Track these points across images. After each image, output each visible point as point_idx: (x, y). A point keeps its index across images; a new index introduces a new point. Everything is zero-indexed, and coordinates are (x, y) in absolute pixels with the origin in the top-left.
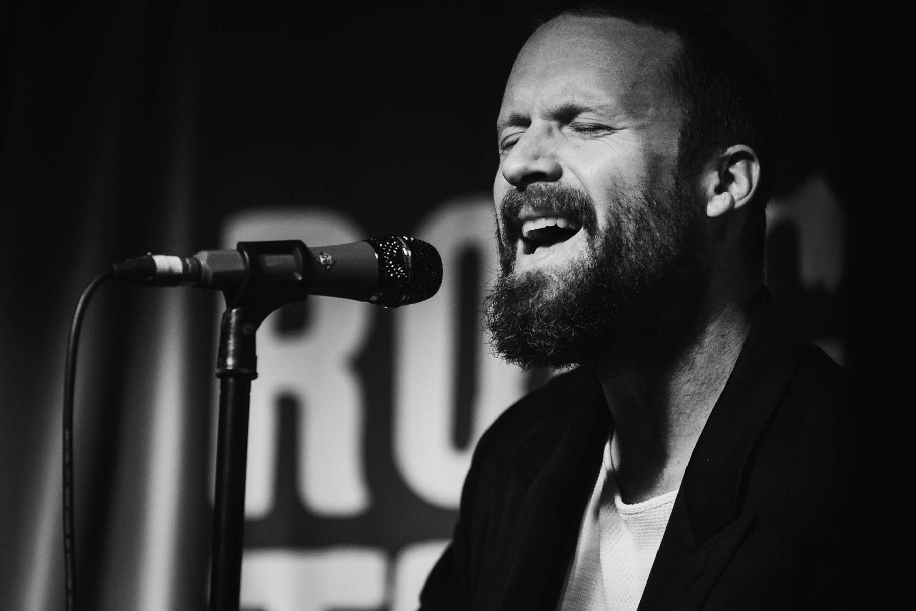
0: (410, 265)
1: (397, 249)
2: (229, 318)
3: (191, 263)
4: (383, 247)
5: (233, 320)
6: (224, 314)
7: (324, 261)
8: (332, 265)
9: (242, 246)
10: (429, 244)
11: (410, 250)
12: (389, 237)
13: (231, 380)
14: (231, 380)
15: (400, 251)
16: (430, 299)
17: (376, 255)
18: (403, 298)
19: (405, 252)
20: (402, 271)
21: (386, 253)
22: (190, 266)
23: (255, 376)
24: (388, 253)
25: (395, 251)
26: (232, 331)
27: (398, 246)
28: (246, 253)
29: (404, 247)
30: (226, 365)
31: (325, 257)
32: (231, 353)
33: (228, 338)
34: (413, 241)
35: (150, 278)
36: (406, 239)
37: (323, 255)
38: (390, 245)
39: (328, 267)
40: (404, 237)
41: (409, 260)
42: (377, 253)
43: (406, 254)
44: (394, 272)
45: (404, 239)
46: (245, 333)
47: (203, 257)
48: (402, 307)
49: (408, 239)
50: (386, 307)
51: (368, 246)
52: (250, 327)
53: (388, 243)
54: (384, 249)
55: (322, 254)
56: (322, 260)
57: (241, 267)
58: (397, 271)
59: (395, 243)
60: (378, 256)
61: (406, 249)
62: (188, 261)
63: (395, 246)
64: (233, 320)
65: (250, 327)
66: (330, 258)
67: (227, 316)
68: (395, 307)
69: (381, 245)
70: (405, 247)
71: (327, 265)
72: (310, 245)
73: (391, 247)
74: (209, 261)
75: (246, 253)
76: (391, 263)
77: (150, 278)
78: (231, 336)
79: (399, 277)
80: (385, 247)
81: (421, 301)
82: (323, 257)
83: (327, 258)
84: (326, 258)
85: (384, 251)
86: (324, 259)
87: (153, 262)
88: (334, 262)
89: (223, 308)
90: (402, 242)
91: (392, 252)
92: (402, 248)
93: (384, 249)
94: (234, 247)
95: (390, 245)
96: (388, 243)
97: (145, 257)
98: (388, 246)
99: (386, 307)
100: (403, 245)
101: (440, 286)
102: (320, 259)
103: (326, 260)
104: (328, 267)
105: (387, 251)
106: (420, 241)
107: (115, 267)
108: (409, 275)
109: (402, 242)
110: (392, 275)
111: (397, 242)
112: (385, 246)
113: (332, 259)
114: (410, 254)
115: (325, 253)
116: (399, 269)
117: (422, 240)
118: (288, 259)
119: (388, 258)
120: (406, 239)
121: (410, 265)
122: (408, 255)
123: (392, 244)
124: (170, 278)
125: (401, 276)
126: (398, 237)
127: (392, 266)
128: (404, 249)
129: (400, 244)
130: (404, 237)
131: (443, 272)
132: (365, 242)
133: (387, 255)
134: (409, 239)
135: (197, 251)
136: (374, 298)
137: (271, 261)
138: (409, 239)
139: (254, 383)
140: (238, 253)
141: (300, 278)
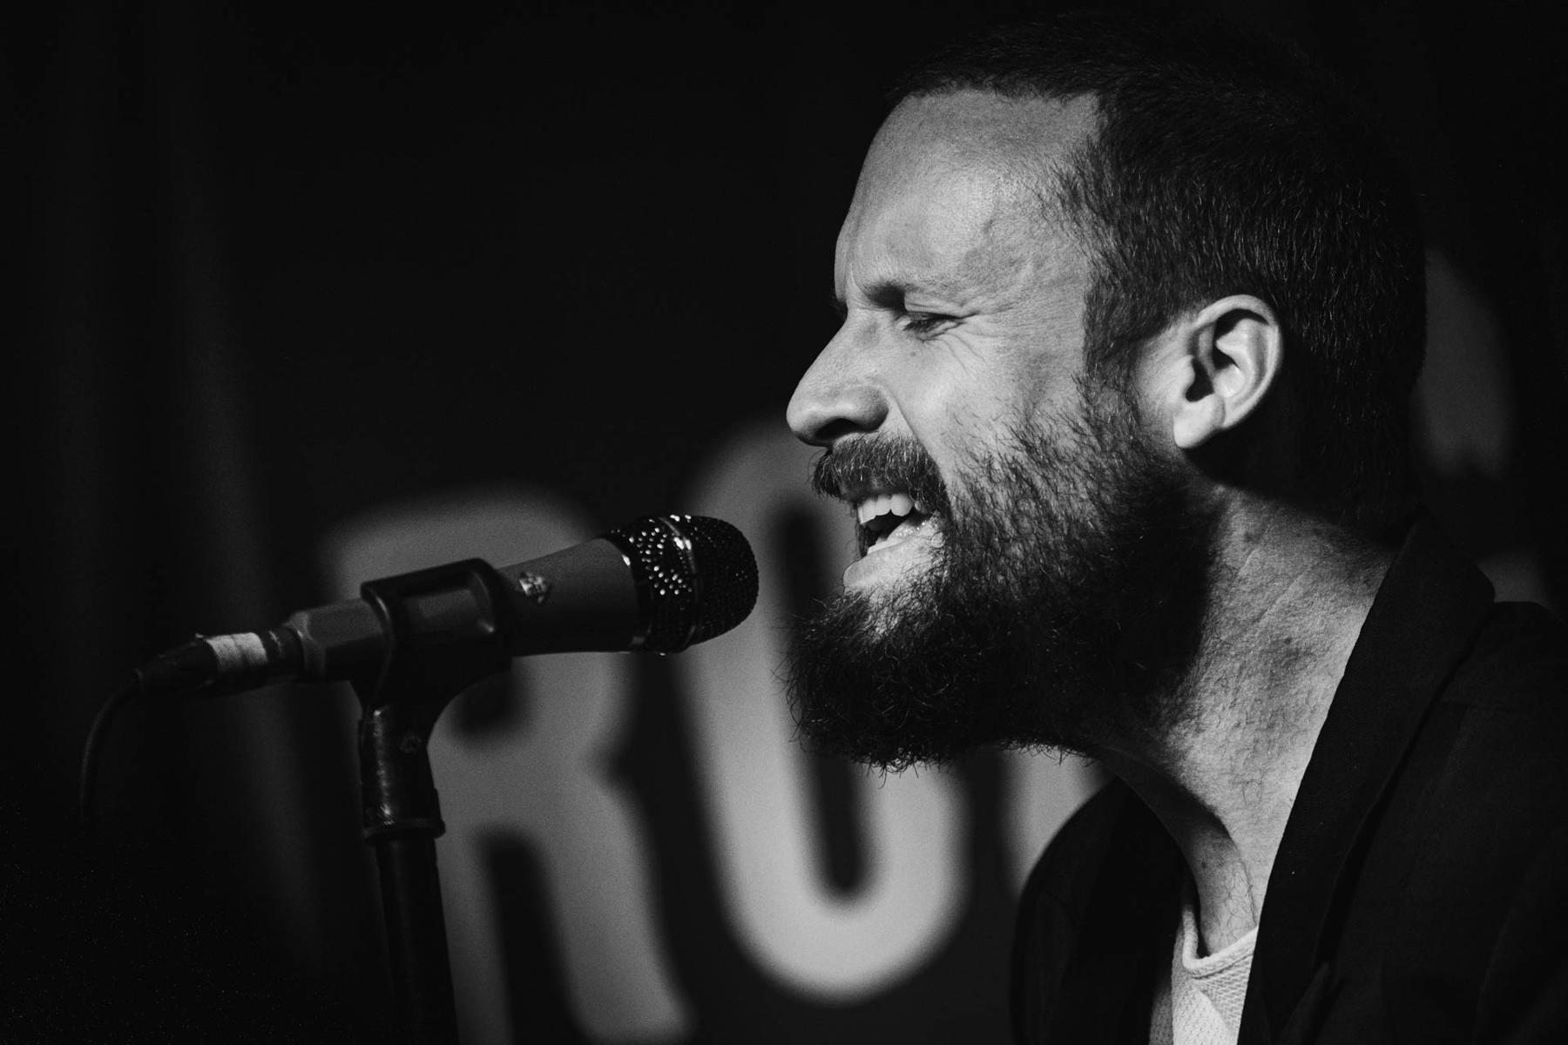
0: (693, 567)
1: (662, 541)
2: (371, 728)
3: (281, 639)
4: (636, 541)
5: (379, 732)
6: (361, 723)
7: (530, 589)
8: (547, 594)
9: (371, 590)
10: (721, 521)
11: (687, 538)
12: (645, 522)
13: (395, 846)
14: (395, 846)
15: (670, 544)
16: (743, 623)
17: (627, 561)
18: (693, 630)
19: (679, 543)
20: (680, 581)
21: (644, 553)
22: (279, 644)
23: (440, 828)
24: (648, 552)
25: (660, 546)
26: (380, 752)
27: (665, 536)
28: (380, 602)
29: (675, 536)
30: (384, 818)
31: (530, 580)
32: (386, 794)
33: (376, 767)
34: (691, 520)
35: (209, 682)
36: (677, 519)
37: (527, 577)
38: (649, 535)
39: (540, 599)
40: (672, 516)
41: (690, 558)
42: (627, 556)
43: (682, 548)
44: (665, 587)
45: (674, 520)
46: (407, 751)
47: (302, 624)
48: (692, 647)
49: (681, 518)
50: (662, 654)
51: (604, 545)
52: (413, 738)
53: (644, 534)
54: (639, 546)
55: (523, 576)
56: (526, 587)
57: (375, 628)
58: (671, 582)
59: (657, 530)
60: (631, 560)
61: (681, 538)
62: (274, 637)
63: (659, 536)
64: (379, 732)
65: (413, 738)
66: (539, 581)
67: (366, 727)
68: (682, 650)
69: (631, 540)
70: (678, 534)
71: (537, 596)
72: (497, 565)
73: (651, 540)
74: (314, 628)
75: (380, 602)
76: (656, 569)
77: (209, 682)
78: (381, 763)
79: (676, 592)
80: (640, 542)
81: (726, 631)
82: (527, 582)
83: (535, 583)
84: (532, 583)
85: (640, 549)
86: (530, 586)
87: (209, 648)
88: (550, 587)
89: (357, 711)
90: (672, 527)
91: (655, 549)
92: (673, 537)
93: (639, 546)
94: (356, 594)
95: (649, 535)
96: (644, 534)
97: (193, 644)
98: (646, 539)
99: (662, 654)
100: (672, 532)
101: (752, 608)
102: (521, 587)
103: (534, 586)
104: (540, 599)
105: (645, 548)
106: (704, 518)
107: (140, 674)
108: (695, 585)
109: (672, 527)
110: (662, 592)
111: (660, 529)
112: (640, 540)
113: (544, 582)
114: (689, 547)
115: (529, 574)
116: (674, 579)
117: (706, 516)
118: (465, 595)
119: (649, 561)
120: (677, 519)
121: (693, 567)
122: (686, 548)
123: (653, 534)
124: (245, 672)
125: (681, 590)
126: (662, 519)
127: (661, 575)
128: (676, 540)
129: (668, 531)
130: (672, 516)
131: (758, 568)
132: (601, 540)
133: (647, 556)
134: (683, 519)
135: (287, 615)
136: (638, 640)
137: (431, 607)
138: (683, 519)
139: (440, 842)
140: (367, 606)
141: (491, 629)
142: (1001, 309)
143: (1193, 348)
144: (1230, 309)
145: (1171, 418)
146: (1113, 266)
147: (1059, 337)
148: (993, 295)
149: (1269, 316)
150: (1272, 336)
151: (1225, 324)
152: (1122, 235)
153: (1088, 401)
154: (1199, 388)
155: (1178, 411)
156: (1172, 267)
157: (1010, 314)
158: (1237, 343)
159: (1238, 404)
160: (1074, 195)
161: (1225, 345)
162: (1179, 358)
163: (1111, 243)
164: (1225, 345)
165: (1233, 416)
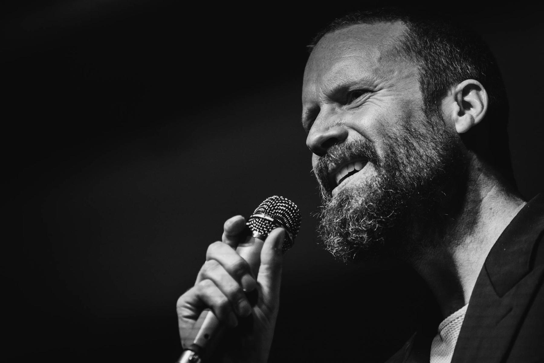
142: (391, 86)
143: (456, 99)
144: (468, 84)
145: (454, 123)
146: (426, 71)
147: (413, 94)
148: (387, 82)
149: (481, 86)
150: (484, 94)
151: (466, 91)
152: (426, 60)
153: (427, 116)
154: (461, 114)
155: (457, 120)
156: (445, 72)
157: (394, 88)
158: (471, 97)
159: (478, 115)
160: (408, 47)
161: (467, 99)
162: (453, 102)
163: (423, 63)
164: (467, 99)
165: (477, 120)
